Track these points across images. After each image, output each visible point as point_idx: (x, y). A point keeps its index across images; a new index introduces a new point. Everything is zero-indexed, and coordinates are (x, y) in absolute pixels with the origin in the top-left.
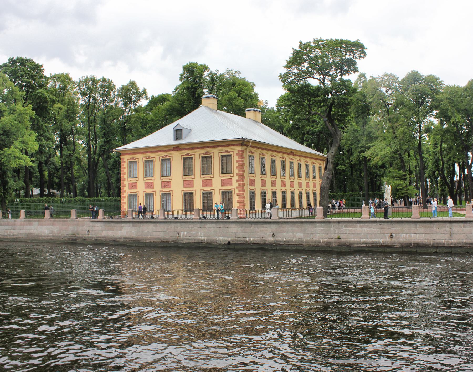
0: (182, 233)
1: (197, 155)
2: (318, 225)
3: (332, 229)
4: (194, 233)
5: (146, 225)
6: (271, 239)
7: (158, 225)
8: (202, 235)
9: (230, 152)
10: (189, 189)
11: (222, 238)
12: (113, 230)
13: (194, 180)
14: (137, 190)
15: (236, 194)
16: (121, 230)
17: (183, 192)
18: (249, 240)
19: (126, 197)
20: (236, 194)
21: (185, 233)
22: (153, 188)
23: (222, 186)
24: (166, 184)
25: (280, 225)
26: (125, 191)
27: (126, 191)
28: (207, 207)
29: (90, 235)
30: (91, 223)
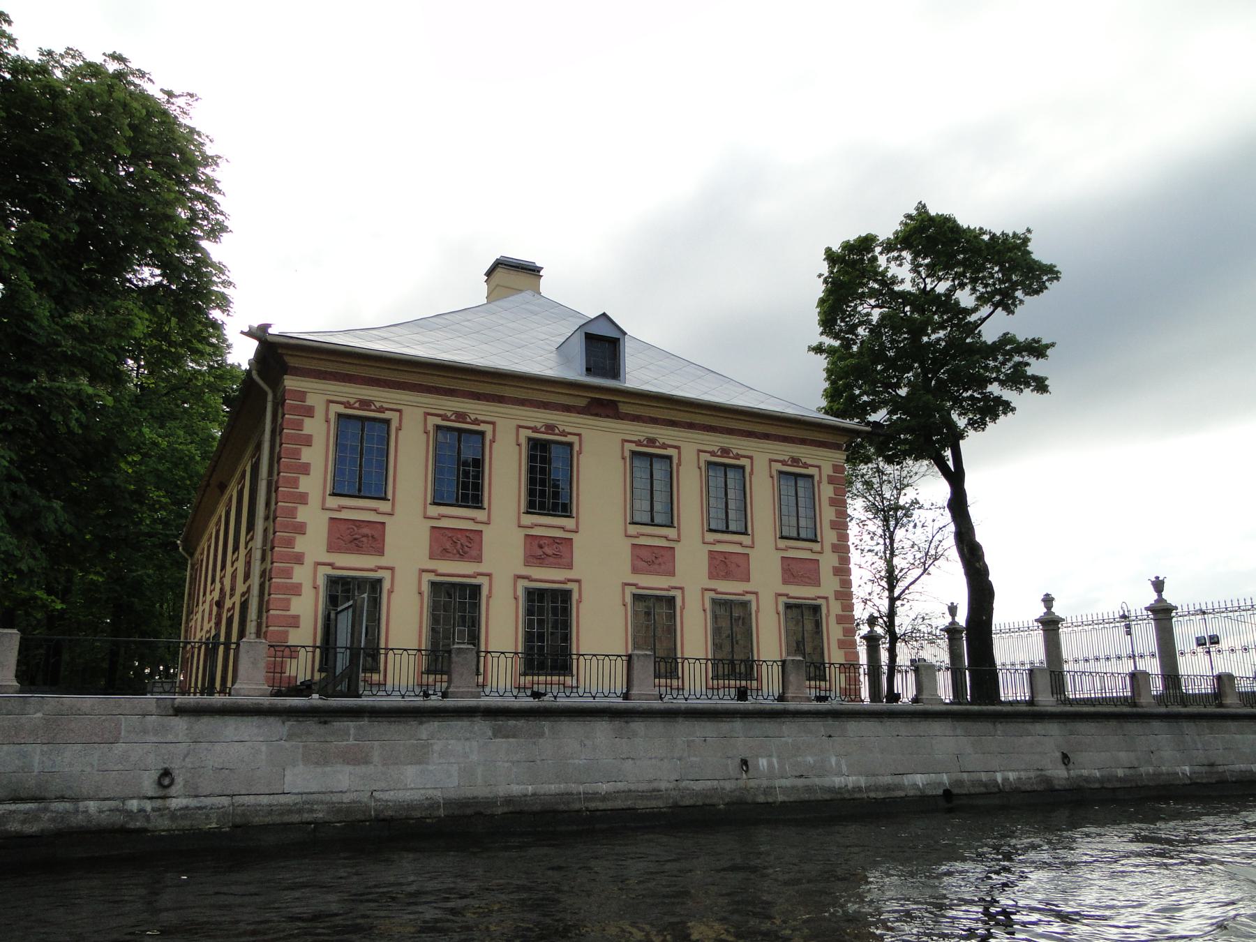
0: (763, 762)
1: (690, 450)
2: (1156, 725)
3: (1188, 738)
4: (810, 759)
5: (571, 730)
6: (1059, 773)
7: (638, 726)
8: (844, 769)
9: (806, 466)
10: (654, 583)
11: (919, 779)
12: (366, 761)
13: (678, 547)
14: (382, 561)
15: (832, 620)
16: (420, 756)
17: (629, 591)
18: (1005, 780)
19: (307, 591)
20: (832, 620)
21: (775, 760)
22: (478, 559)
23: (785, 582)
24: (548, 551)
25: (1071, 726)
26: (299, 559)
27: (309, 561)
28: (734, 661)
29: (174, 803)
30: (180, 723)
